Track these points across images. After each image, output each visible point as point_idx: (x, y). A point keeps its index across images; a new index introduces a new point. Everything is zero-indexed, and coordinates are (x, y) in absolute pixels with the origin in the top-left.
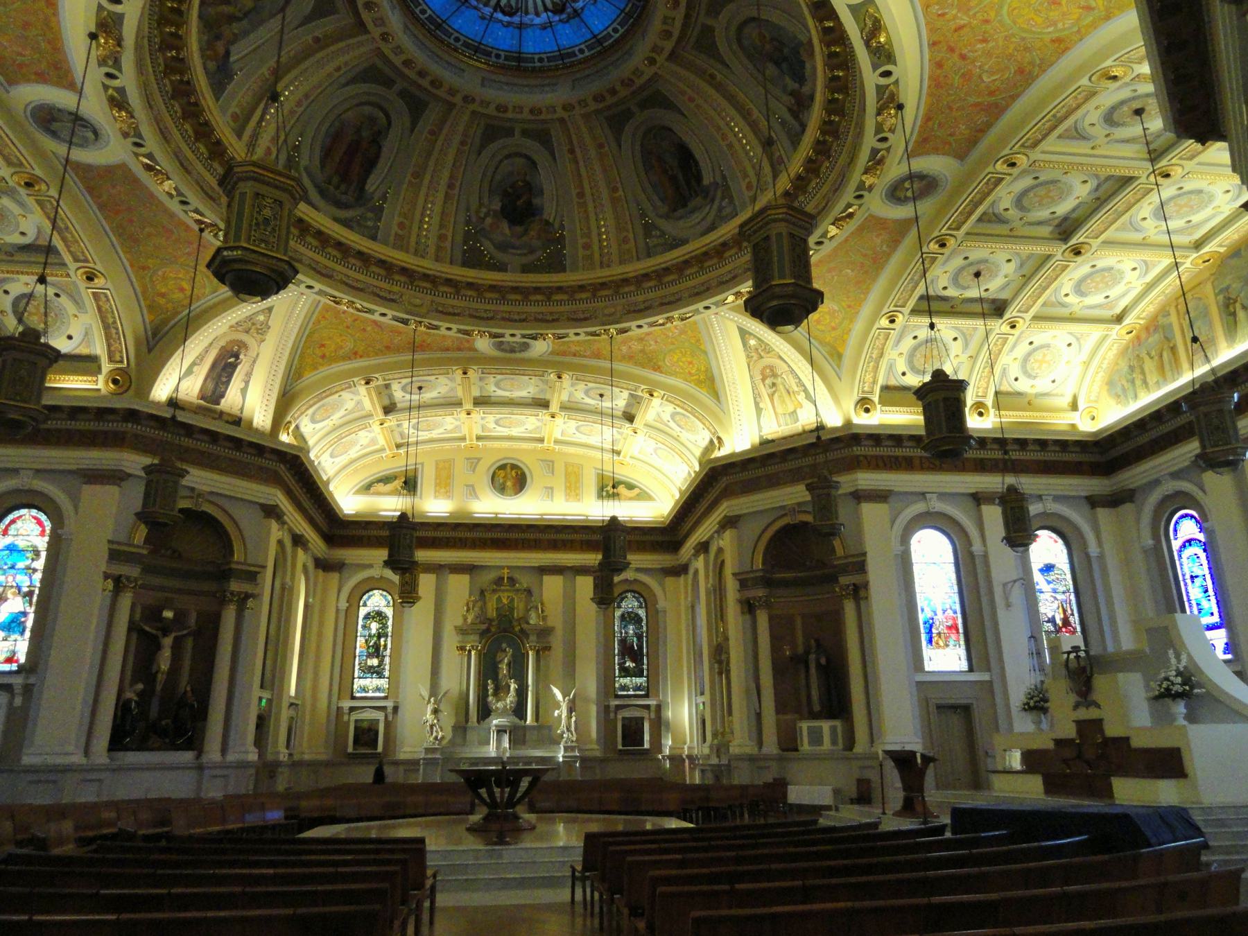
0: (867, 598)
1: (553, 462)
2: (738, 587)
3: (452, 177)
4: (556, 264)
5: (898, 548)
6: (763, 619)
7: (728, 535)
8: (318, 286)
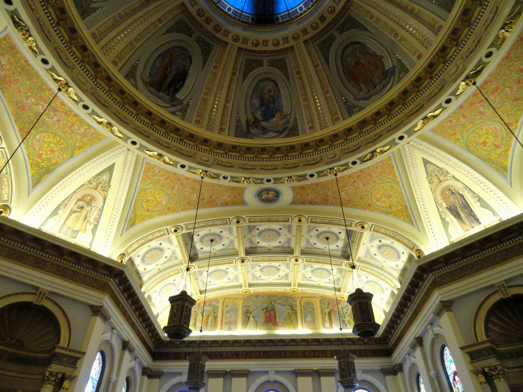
2: (469, 360)
3: (227, 96)
4: (293, 132)
7: (446, 318)
8: (139, 140)
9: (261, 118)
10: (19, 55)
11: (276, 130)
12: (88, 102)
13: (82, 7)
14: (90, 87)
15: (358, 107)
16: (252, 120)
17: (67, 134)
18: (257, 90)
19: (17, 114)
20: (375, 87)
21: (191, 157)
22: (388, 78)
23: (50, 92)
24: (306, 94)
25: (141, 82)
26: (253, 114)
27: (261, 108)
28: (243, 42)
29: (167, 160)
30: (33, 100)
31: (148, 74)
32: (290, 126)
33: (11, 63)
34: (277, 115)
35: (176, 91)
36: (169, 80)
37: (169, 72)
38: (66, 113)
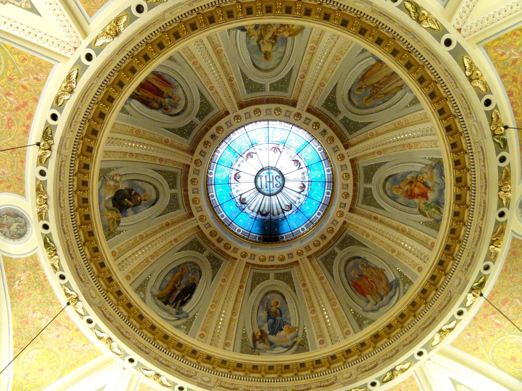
3: (234, 309)
9: (268, 332)
10: (40, 272)
11: (284, 344)
12: (93, 316)
13: (109, 230)
14: (99, 301)
15: (368, 319)
16: (259, 334)
17: (63, 350)
18: (264, 302)
19: (18, 328)
20: (382, 299)
21: (191, 377)
22: (394, 289)
23: (59, 306)
24: (313, 306)
25: (150, 295)
26: (260, 327)
27: (268, 320)
28: (250, 258)
29: (165, 382)
30: (39, 314)
31: (157, 287)
32: (299, 340)
33: (30, 279)
34: (285, 328)
35: (183, 303)
36: (178, 292)
37: (179, 286)
38: (68, 328)
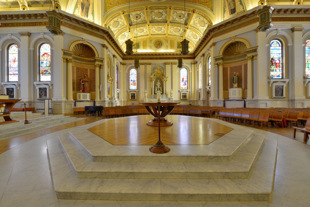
0: (256, 59)
1: (167, 40)
5: (267, 45)
6: (221, 68)
